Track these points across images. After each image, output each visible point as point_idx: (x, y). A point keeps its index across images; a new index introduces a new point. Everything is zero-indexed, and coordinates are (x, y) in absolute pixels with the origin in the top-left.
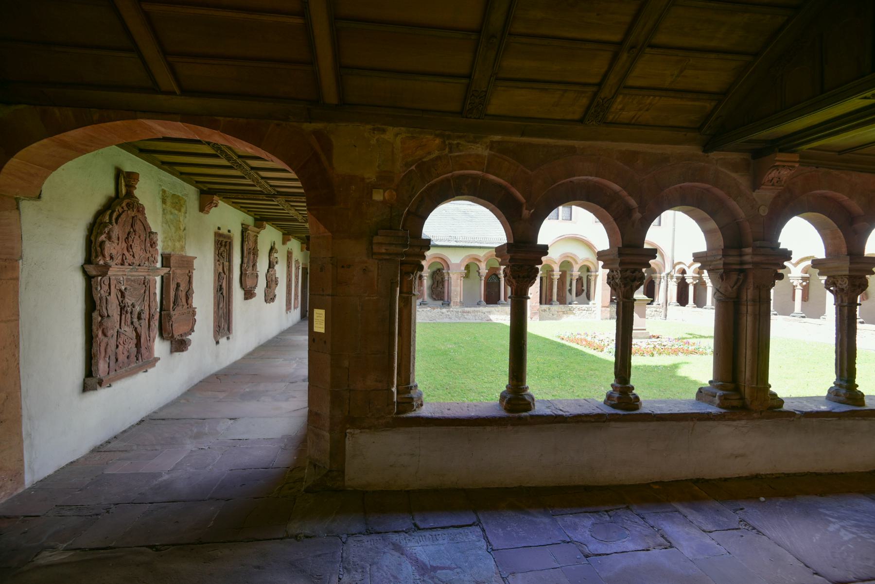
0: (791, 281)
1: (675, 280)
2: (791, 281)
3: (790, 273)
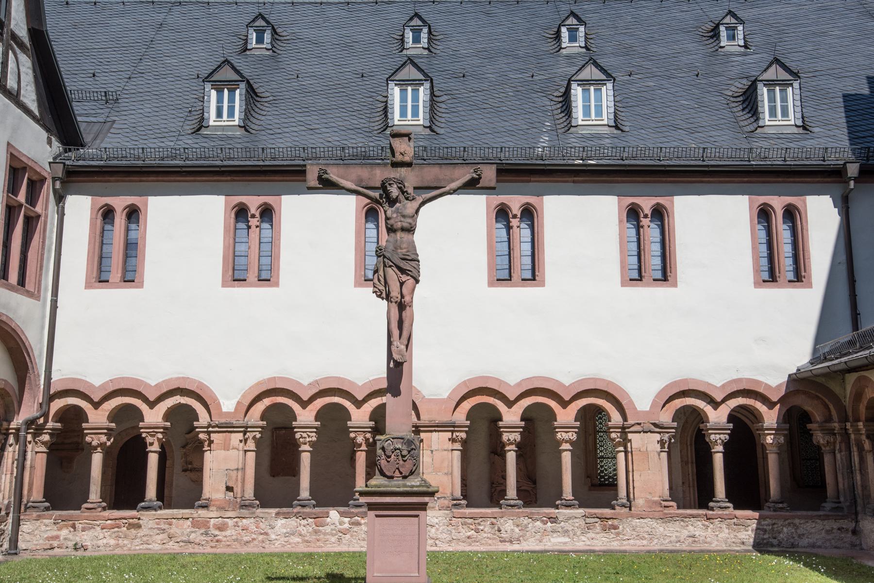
0: (352, 435)
1: (46, 438)
2: (352, 435)
3: (350, 420)
